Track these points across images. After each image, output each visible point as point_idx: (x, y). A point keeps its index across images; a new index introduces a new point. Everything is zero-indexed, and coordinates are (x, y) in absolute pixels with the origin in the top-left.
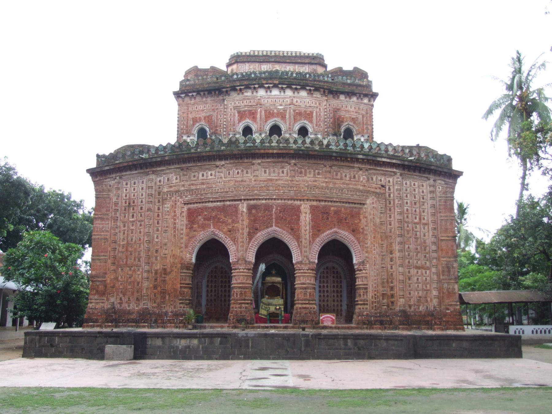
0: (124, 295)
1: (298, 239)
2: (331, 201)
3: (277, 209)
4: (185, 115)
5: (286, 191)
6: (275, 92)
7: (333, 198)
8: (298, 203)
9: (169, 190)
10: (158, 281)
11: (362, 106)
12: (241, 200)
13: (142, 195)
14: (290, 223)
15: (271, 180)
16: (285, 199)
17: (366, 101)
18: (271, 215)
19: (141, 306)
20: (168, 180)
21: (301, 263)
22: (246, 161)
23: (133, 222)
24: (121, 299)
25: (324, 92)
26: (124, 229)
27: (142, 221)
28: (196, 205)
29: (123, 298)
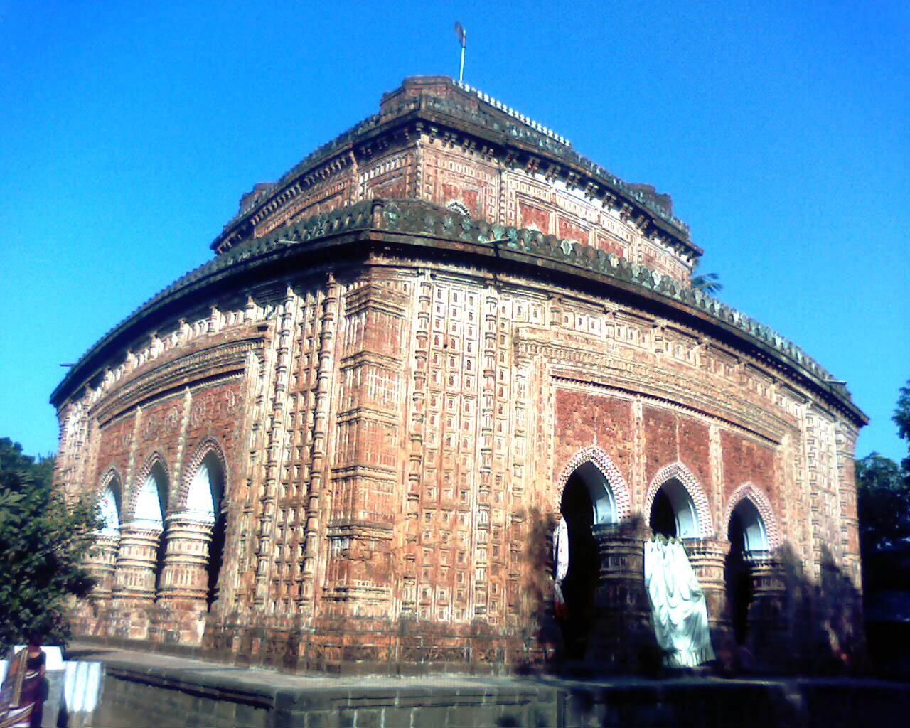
0: (433, 586)
1: (709, 491)
2: (744, 428)
3: (681, 427)
4: (431, 171)
5: (698, 394)
6: (579, 193)
7: (748, 423)
8: (706, 419)
9: (532, 336)
10: (501, 554)
11: (678, 264)
12: (634, 393)
13: (470, 332)
14: (696, 459)
15: (680, 366)
16: (692, 409)
17: (684, 258)
18: (674, 437)
19: (468, 617)
20: (519, 309)
21: (715, 539)
22: (648, 316)
23: (453, 394)
24: (424, 593)
25: (644, 221)
26: (433, 408)
27: (472, 398)
28: (570, 385)
29: (429, 591)
